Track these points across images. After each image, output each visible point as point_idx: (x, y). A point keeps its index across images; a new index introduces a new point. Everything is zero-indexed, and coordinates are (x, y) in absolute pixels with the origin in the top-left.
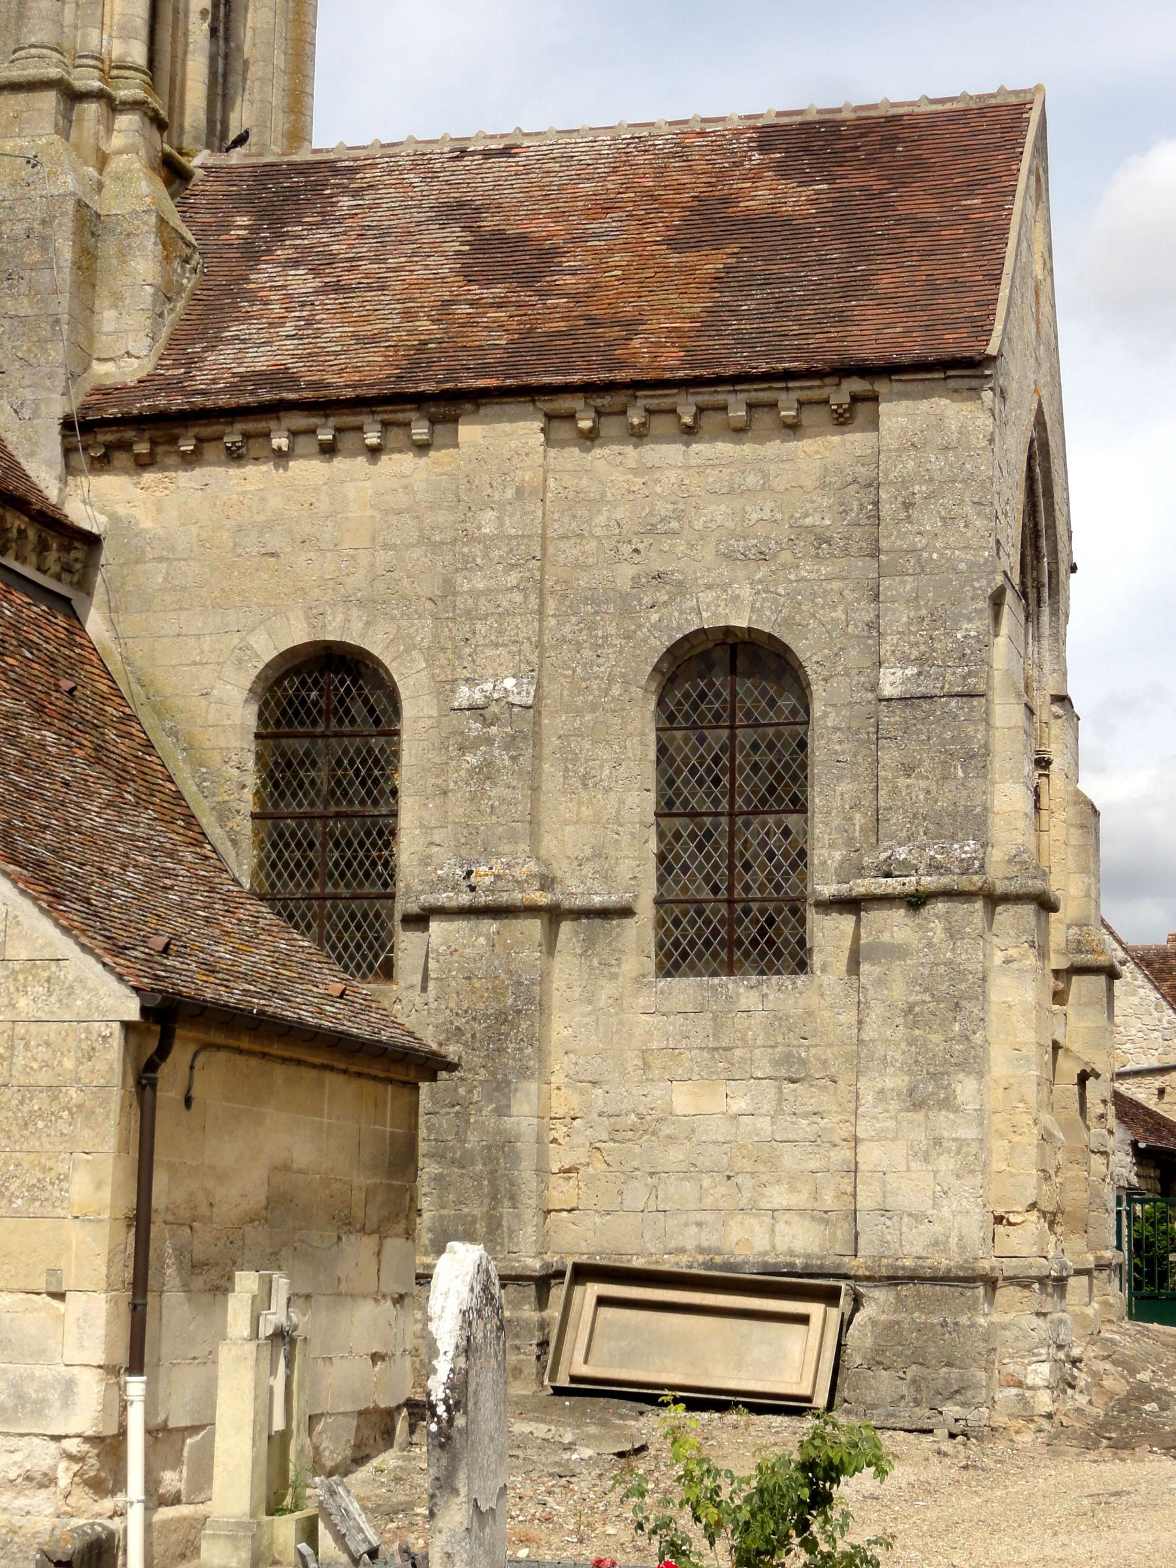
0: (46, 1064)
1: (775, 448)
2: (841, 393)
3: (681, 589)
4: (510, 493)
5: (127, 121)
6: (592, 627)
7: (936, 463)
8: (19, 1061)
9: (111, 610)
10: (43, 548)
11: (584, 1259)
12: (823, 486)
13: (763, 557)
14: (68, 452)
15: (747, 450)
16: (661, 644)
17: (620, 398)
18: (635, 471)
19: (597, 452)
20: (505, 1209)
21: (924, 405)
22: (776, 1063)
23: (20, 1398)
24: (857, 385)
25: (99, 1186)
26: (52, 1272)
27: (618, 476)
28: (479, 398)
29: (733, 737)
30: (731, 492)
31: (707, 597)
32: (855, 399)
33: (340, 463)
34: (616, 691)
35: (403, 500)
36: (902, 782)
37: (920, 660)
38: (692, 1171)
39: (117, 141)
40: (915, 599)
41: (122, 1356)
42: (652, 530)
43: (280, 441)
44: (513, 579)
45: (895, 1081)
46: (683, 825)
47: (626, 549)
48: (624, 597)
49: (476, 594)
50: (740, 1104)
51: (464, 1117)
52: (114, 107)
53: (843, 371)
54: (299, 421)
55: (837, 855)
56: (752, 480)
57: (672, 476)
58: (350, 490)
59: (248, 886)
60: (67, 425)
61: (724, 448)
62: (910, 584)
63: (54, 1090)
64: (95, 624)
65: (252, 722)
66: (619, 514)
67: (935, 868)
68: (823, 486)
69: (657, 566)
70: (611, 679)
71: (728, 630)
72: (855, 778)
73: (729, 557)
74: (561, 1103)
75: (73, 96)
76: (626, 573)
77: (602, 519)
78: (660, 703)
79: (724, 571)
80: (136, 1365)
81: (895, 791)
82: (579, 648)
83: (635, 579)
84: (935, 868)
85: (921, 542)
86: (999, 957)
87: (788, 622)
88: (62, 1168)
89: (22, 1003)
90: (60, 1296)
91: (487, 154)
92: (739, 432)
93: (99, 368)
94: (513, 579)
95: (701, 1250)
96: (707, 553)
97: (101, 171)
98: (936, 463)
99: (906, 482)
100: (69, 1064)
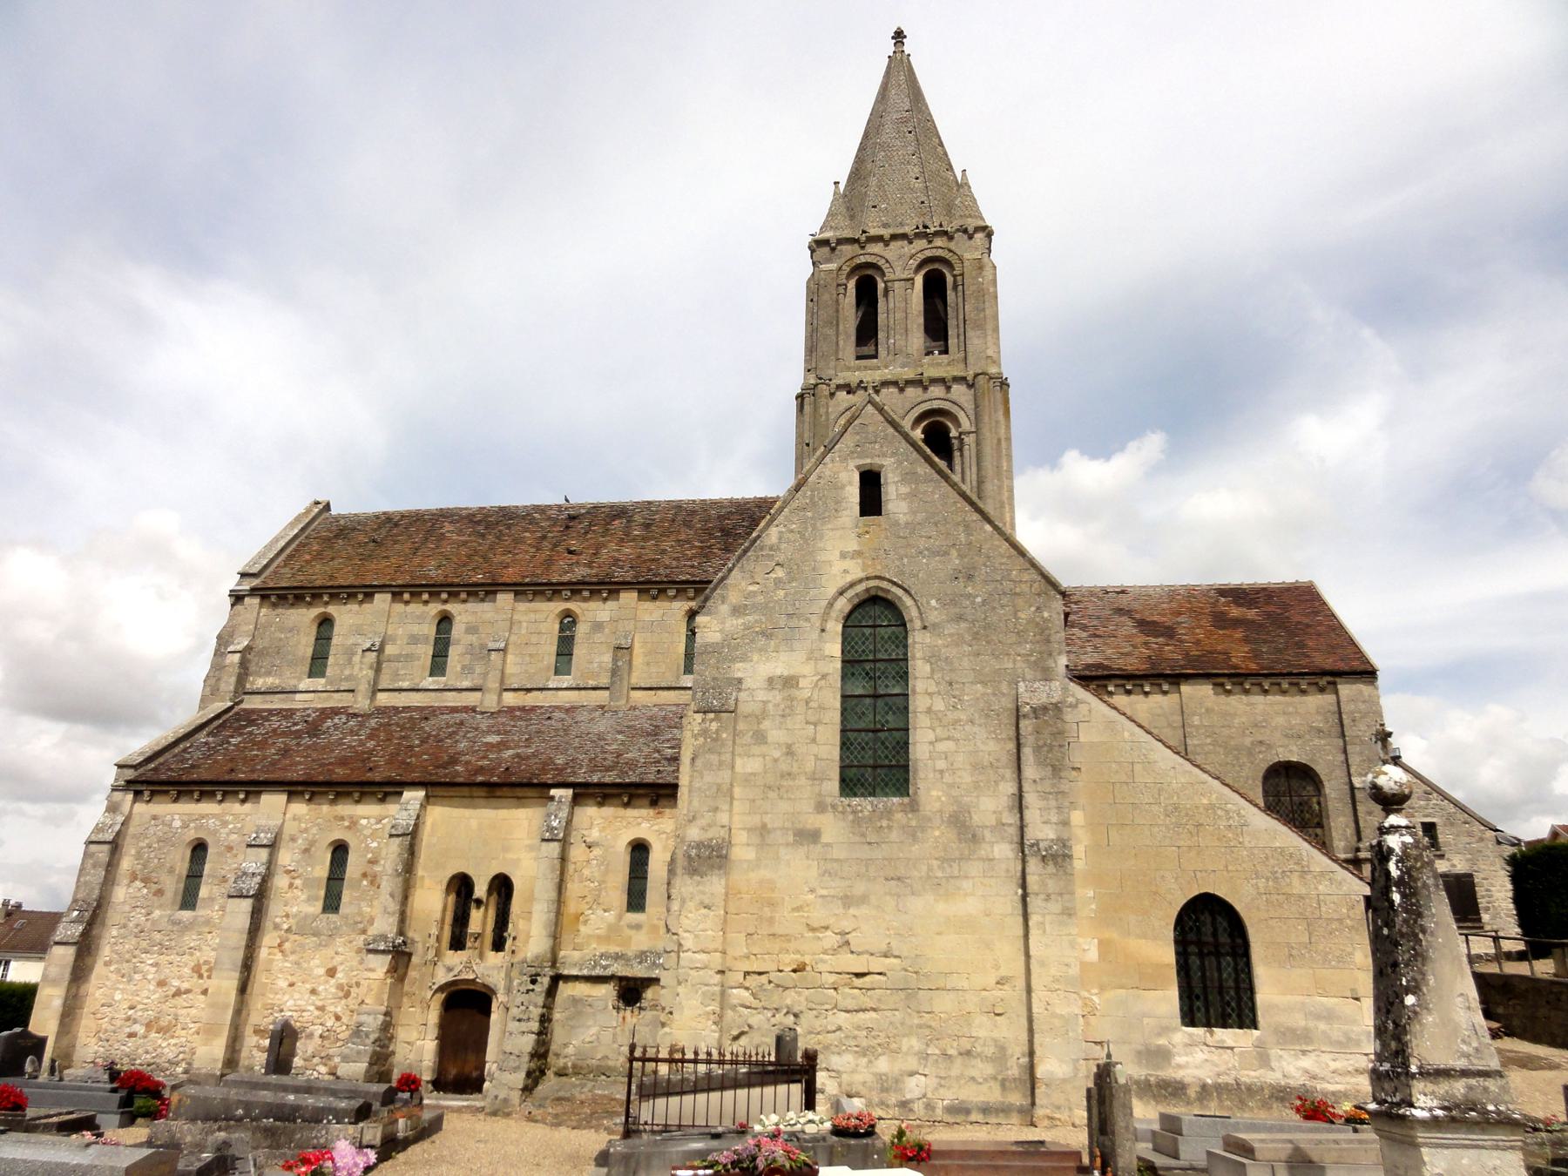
0: (1335, 911)
1: (1298, 699)
2: (1323, 682)
3: (1269, 747)
4: (1203, 710)
6: (1238, 759)
7: (1362, 707)
8: (1323, 909)
12: (1318, 713)
15: (1287, 699)
16: (1265, 766)
17: (1241, 679)
18: (1247, 705)
19: (1232, 697)
21: (1354, 687)
23: (1349, 1039)
24: (1330, 679)
25: (1366, 956)
26: (1352, 990)
27: (1242, 707)
28: (1187, 677)
29: (1291, 800)
30: (1284, 713)
31: (1280, 750)
32: (1329, 683)
33: (1133, 697)
34: (1250, 782)
35: (1159, 711)
36: (1368, 818)
40: (1361, 753)
42: (1256, 725)
44: (1209, 741)
47: (1247, 732)
48: (1249, 749)
49: (1195, 746)
53: (1324, 673)
54: (1119, 682)
55: (1342, 844)
56: (1291, 709)
57: (1261, 707)
58: (1138, 706)
61: (1279, 698)
62: (1358, 748)
63: (1340, 921)
66: (1244, 720)
68: (1318, 713)
69: (1260, 739)
70: (1248, 778)
71: (1289, 762)
72: (1345, 816)
73: (1286, 736)
76: (1248, 741)
77: (1236, 721)
79: (1286, 741)
81: (1366, 821)
82: (1234, 765)
83: (1252, 743)
85: (1360, 733)
87: (1312, 760)
88: (1349, 949)
89: (1320, 887)
90: (1357, 999)
91: (1118, 593)
92: (1284, 692)
94: (1209, 741)
96: (1278, 735)
98: (1362, 707)
99: (1352, 712)
100: (1344, 911)
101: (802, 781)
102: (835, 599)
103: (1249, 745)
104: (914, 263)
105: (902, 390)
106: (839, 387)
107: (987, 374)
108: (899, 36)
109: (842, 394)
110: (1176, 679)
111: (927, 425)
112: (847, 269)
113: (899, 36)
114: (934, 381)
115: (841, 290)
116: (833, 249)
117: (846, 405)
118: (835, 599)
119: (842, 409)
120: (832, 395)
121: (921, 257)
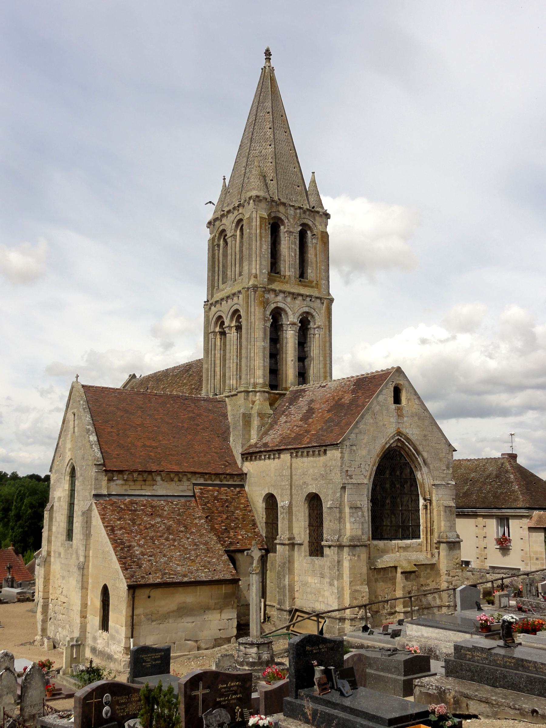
2: (322, 449)
3: (307, 485)
5: (258, 394)
9: (248, 486)
10: (233, 478)
11: (297, 608)
13: (317, 479)
14: (242, 458)
20: (285, 598)
22: (320, 574)
24: (324, 448)
37: (333, 500)
38: (311, 593)
39: (257, 398)
41: (130, 635)
43: (263, 457)
45: (328, 580)
46: (311, 527)
50: (316, 581)
51: (280, 580)
52: (256, 392)
54: (265, 454)
59: (264, 535)
60: (242, 455)
64: (246, 488)
65: (264, 506)
67: (332, 541)
74: (296, 578)
75: (248, 392)
78: (309, 505)
80: (132, 637)
84: (332, 541)
86: (344, 557)
93: (252, 441)
95: (312, 608)
97: (253, 405)
101: (60, 536)
102: (66, 468)
103: (301, 484)
104: (234, 225)
105: (227, 302)
106: (211, 304)
107: (246, 288)
108: (268, 53)
109: (213, 307)
110: (280, 451)
111: (236, 318)
112: (217, 235)
113: (268, 53)
114: (234, 294)
115: (216, 248)
116: (214, 225)
117: (213, 313)
118: (66, 468)
119: (212, 316)
120: (210, 308)
121: (236, 220)
